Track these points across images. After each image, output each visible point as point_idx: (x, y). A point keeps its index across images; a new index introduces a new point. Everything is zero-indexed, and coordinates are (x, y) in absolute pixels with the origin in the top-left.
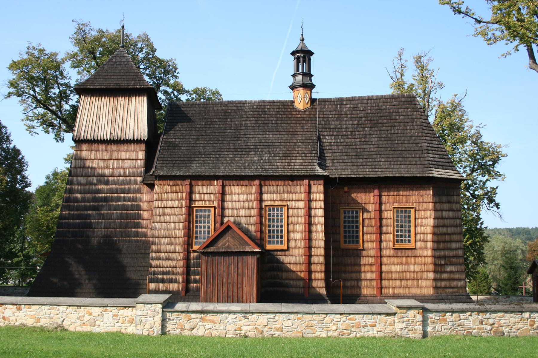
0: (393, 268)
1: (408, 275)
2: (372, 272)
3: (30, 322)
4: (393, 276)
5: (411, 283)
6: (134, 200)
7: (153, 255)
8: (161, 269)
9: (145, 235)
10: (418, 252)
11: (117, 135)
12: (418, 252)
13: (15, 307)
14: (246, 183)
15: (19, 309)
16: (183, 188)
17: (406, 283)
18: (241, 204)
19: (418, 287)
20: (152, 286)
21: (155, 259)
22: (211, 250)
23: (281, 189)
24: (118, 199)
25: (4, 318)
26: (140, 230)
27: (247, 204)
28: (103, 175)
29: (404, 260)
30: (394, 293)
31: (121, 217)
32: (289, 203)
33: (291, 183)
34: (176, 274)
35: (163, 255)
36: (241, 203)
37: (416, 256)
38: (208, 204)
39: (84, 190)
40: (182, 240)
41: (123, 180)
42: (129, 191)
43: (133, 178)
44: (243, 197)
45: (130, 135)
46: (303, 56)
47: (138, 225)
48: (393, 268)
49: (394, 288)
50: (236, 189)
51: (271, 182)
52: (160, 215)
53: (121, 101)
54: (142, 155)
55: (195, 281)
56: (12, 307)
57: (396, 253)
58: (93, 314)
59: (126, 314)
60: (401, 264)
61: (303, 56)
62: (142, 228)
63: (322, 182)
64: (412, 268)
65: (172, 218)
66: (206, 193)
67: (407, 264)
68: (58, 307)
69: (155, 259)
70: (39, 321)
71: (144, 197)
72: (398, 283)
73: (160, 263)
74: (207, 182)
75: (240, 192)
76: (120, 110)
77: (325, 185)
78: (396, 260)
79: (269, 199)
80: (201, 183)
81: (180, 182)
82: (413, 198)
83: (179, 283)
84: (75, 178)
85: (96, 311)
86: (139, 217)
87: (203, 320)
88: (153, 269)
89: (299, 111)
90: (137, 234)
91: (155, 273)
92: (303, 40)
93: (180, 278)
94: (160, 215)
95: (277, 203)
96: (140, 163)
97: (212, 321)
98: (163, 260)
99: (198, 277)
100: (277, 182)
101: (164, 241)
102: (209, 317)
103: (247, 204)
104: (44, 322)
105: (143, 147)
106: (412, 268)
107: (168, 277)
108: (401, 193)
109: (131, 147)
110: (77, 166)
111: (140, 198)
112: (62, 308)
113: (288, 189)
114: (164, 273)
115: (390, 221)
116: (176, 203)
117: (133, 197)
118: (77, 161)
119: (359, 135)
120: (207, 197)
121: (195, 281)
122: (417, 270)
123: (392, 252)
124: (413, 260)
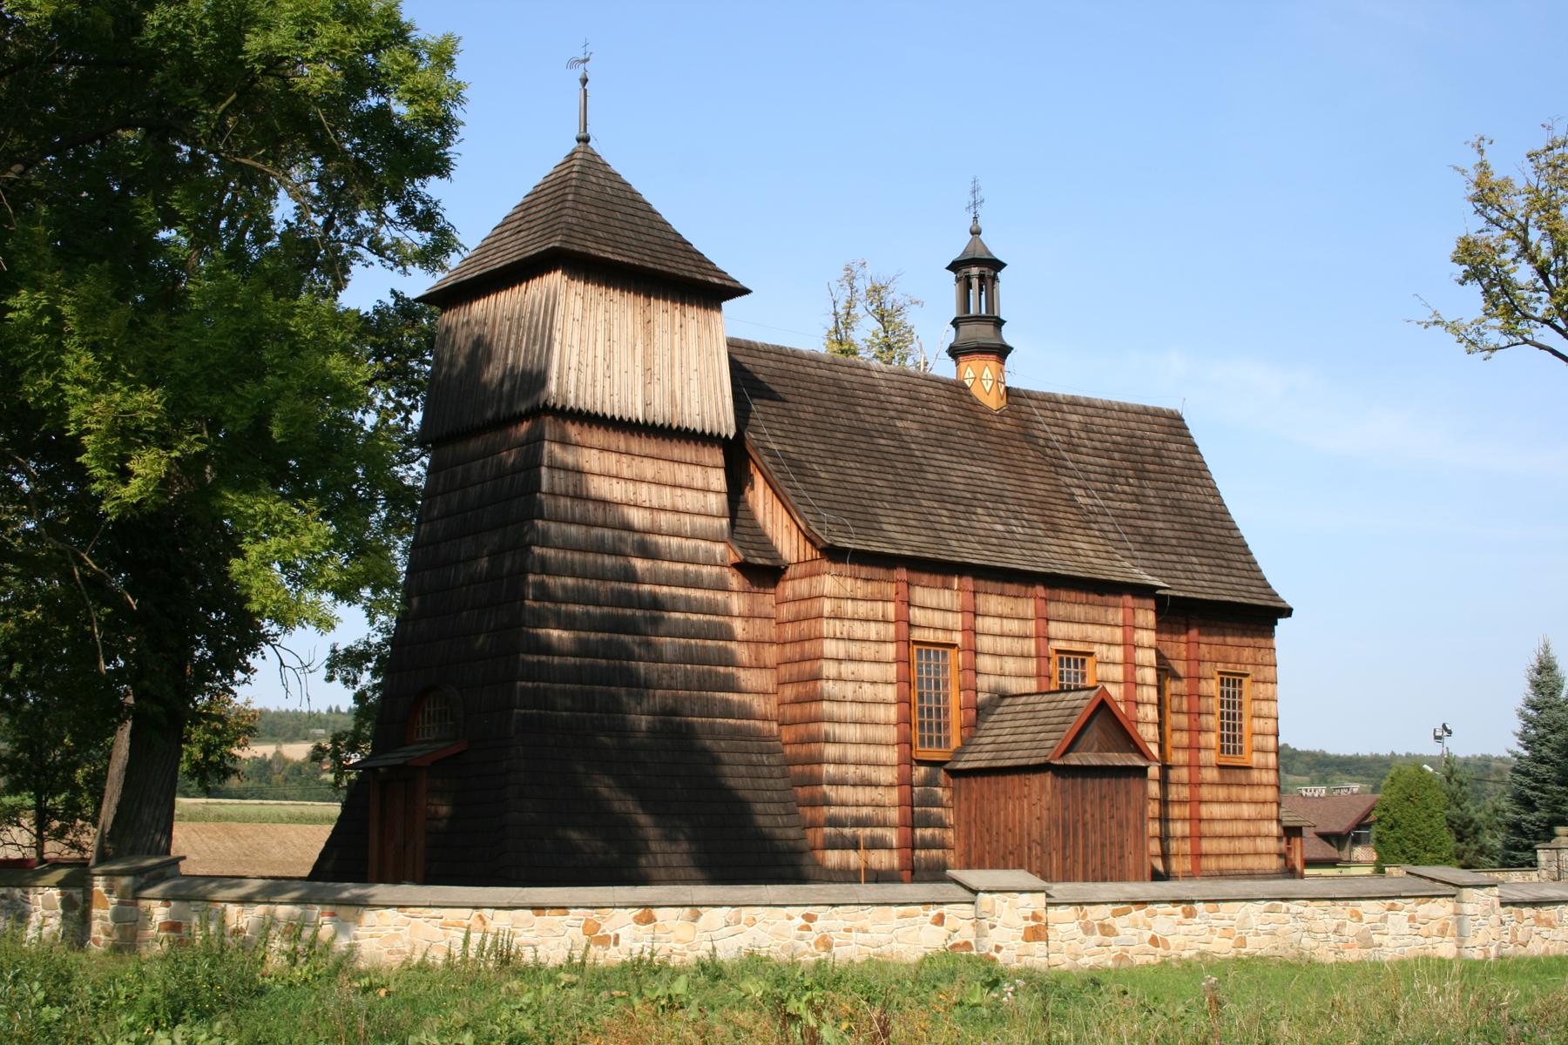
0: (1217, 810)
1: (1240, 828)
2: (1184, 820)
3: (1222, 947)
4: (1218, 828)
5: (1245, 845)
6: (712, 609)
7: (830, 770)
8: (852, 811)
9: (748, 714)
10: (1255, 775)
11: (660, 413)
12: (1255, 775)
13: (1179, 909)
14: (1012, 588)
15: (1190, 914)
16: (890, 589)
17: (1238, 845)
18: (1005, 644)
19: (1256, 854)
20: (833, 858)
21: (835, 783)
22: (1074, 760)
23: (1079, 611)
24: (690, 606)
25: (1154, 941)
26: (735, 697)
27: (1017, 646)
28: (628, 527)
29: (1234, 791)
30: (1220, 870)
31: (688, 657)
32: (1096, 649)
33: (1097, 598)
34: (884, 824)
35: (851, 772)
36: (1005, 642)
37: (1251, 785)
38: (941, 637)
39: (584, 564)
40: (892, 734)
41: (680, 548)
42: (697, 583)
43: (703, 544)
44: (1014, 626)
45: (692, 418)
46: (977, 270)
47: (731, 685)
48: (1217, 810)
49: (1219, 855)
50: (993, 603)
51: (1063, 594)
52: (839, 660)
53: (663, 312)
54: (718, 479)
55: (927, 845)
56: (1169, 908)
57: (1222, 776)
58: (1365, 917)
59: (1432, 915)
60: (1229, 801)
61: (977, 270)
62: (739, 691)
63: (1151, 603)
64: (1247, 810)
65: (867, 670)
66: (938, 607)
67: (1240, 802)
68: (1285, 904)
69: (835, 783)
70: (1242, 942)
71: (737, 603)
72: (1225, 846)
73: (846, 793)
74: (939, 579)
75: (1007, 611)
76: (661, 339)
77: (1158, 613)
78: (1222, 793)
79: (1060, 635)
80: (925, 578)
81: (880, 573)
82: (1247, 654)
83: (891, 848)
84: (553, 526)
85: (1371, 909)
86: (729, 660)
87: (1538, 920)
88: (833, 810)
89: (988, 411)
90: (728, 711)
91: (835, 822)
92: (976, 232)
93: (892, 835)
94: (839, 660)
95: (1077, 647)
96: (716, 502)
97: (1549, 924)
98: (854, 785)
99: (928, 832)
100: (1073, 595)
101: (853, 732)
102: (1545, 912)
103: (1017, 646)
104: (1258, 945)
105: (718, 457)
106: (1247, 810)
107: (868, 831)
108: (1229, 640)
109: (688, 452)
110: (557, 490)
111: (726, 606)
112: (1294, 907)
113: (1094, 613)
114: (860, 823)
115: (1214, 704)
116: (873, 630)
117: (709, 601)
118: (556, 473)
119: (1124, 493)
120: (937, 618)
121: (927, 845)
122: (1253, 815)
123: (1211, 775)
124: (1246, 793)
